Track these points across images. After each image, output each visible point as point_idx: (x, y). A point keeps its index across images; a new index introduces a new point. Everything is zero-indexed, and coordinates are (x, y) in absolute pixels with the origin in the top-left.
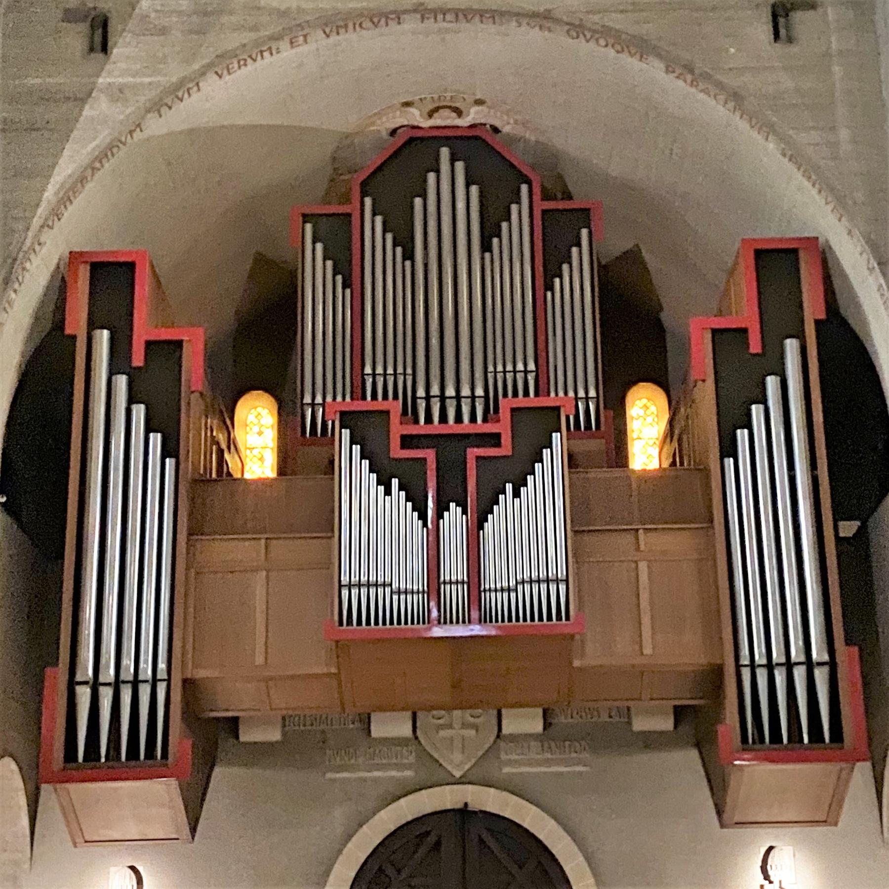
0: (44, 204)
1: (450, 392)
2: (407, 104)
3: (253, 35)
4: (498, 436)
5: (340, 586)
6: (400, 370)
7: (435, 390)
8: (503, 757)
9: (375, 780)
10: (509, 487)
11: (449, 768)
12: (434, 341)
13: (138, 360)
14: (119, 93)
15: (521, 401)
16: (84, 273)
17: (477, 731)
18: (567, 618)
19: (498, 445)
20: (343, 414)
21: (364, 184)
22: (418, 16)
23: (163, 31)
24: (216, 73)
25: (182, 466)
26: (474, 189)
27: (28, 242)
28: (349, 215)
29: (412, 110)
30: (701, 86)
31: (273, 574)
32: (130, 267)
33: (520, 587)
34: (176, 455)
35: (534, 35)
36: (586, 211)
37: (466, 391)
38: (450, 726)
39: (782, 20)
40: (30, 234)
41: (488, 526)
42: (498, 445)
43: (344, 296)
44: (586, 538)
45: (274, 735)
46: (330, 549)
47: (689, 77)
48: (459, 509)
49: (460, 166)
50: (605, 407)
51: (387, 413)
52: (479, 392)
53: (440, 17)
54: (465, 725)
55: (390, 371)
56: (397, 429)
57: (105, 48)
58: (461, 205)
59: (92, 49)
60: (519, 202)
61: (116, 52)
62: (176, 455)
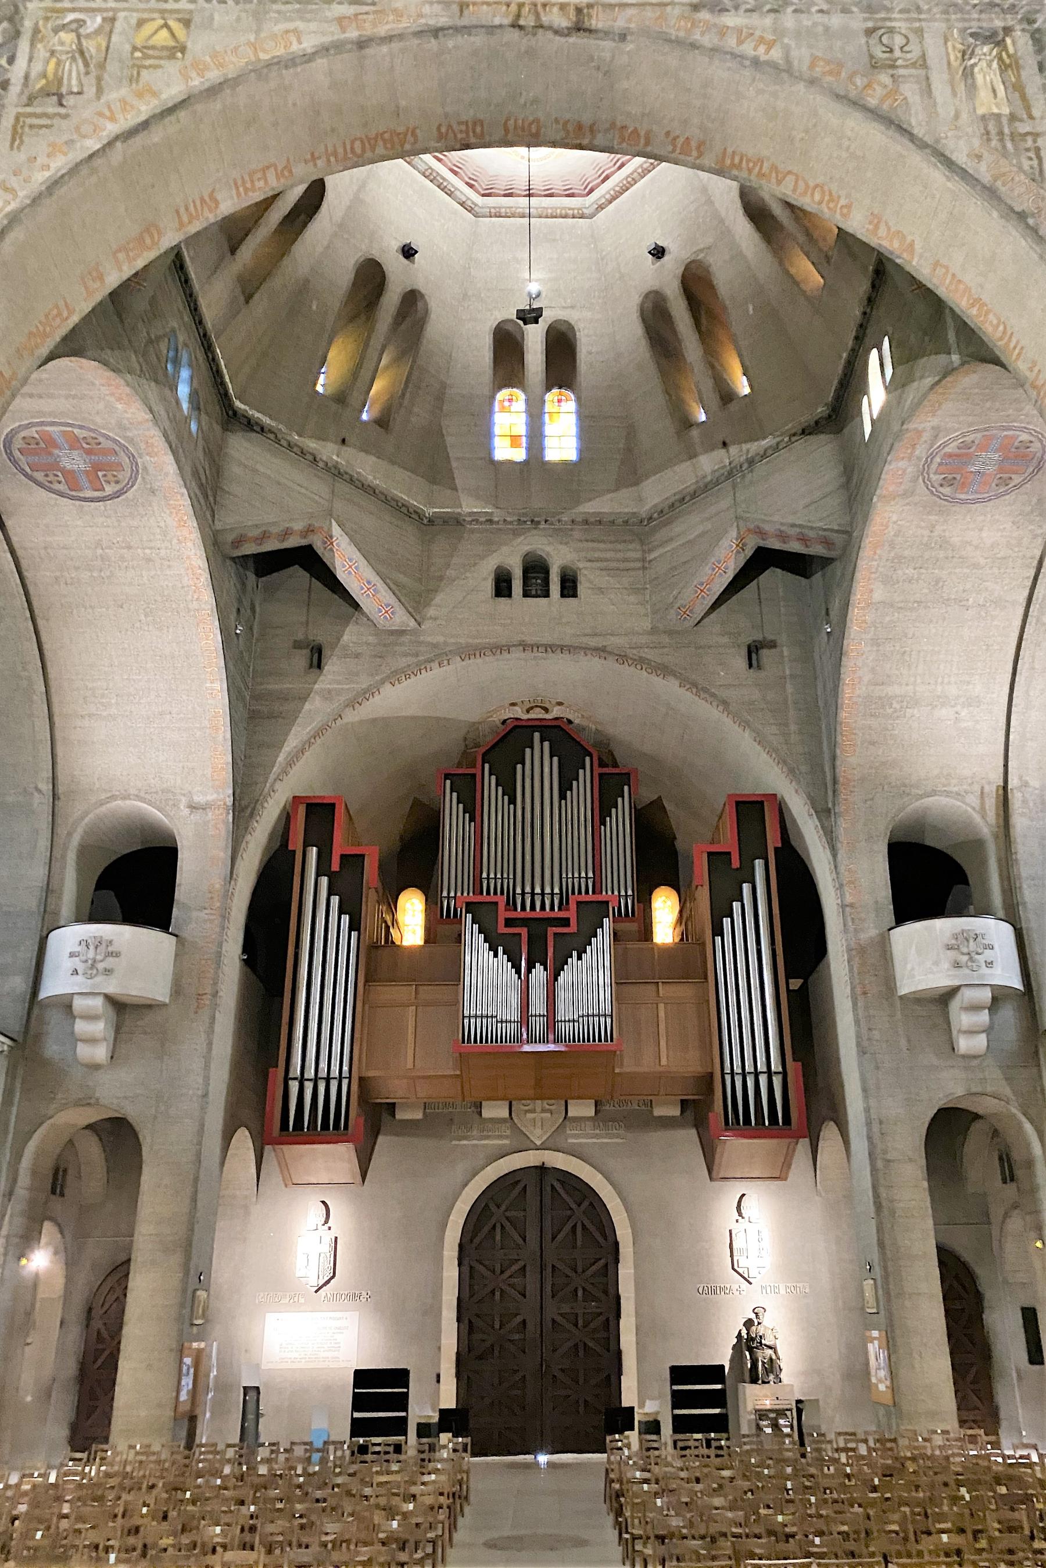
0: (277, 765)
1: (538, 890)
2: (513, 704)
3: (415, 660)
4: (568, 919)
6: (505, 876)
7: (528, 889)
8: (568, 1132)
9: (483, 1146)
10: (575, 953)
11: (532, 1138)
12: (528, 857)
13: (335, 867)
14: (328, 695)
15: (583, 898)
16: (302, 810)
18: (612, 1040)
19: (568, 925)
20: (468, 904)
21: (484, 755)
22: (521, 648)
23: (357, 656)
25: (362, 937)
26: (555, 759)
27: (266, 790)
28: (474, 776)
29: (516, 708)
30: (703, 695)
31: (420, 1009)
32: (333, 805)
33: (581, 1020)
34: (359, 930)
35: (595, 664)
36: (628, 774)
37: (548, 890)
38: (533, 1111)
39: (754, 656)
41: (561, 979)
42: (568, 925)
43: (470, 828)
44: (626, 989)
45: (419, 1115)
46: (457, 992)
47: (694, 690)
48: (542, 967)
49: (546, 744)
50: (638, 902)
51: (496, 903)
52: (557, 890)
53: (535, 649)
54: (543, 1111)
55: (499, 876)
56: (503, 914)
57: (319, 666)
58: (547, 770)
59: (311, 666)
60: (584, 768)
61: (328, 667)
62: (359, 930)
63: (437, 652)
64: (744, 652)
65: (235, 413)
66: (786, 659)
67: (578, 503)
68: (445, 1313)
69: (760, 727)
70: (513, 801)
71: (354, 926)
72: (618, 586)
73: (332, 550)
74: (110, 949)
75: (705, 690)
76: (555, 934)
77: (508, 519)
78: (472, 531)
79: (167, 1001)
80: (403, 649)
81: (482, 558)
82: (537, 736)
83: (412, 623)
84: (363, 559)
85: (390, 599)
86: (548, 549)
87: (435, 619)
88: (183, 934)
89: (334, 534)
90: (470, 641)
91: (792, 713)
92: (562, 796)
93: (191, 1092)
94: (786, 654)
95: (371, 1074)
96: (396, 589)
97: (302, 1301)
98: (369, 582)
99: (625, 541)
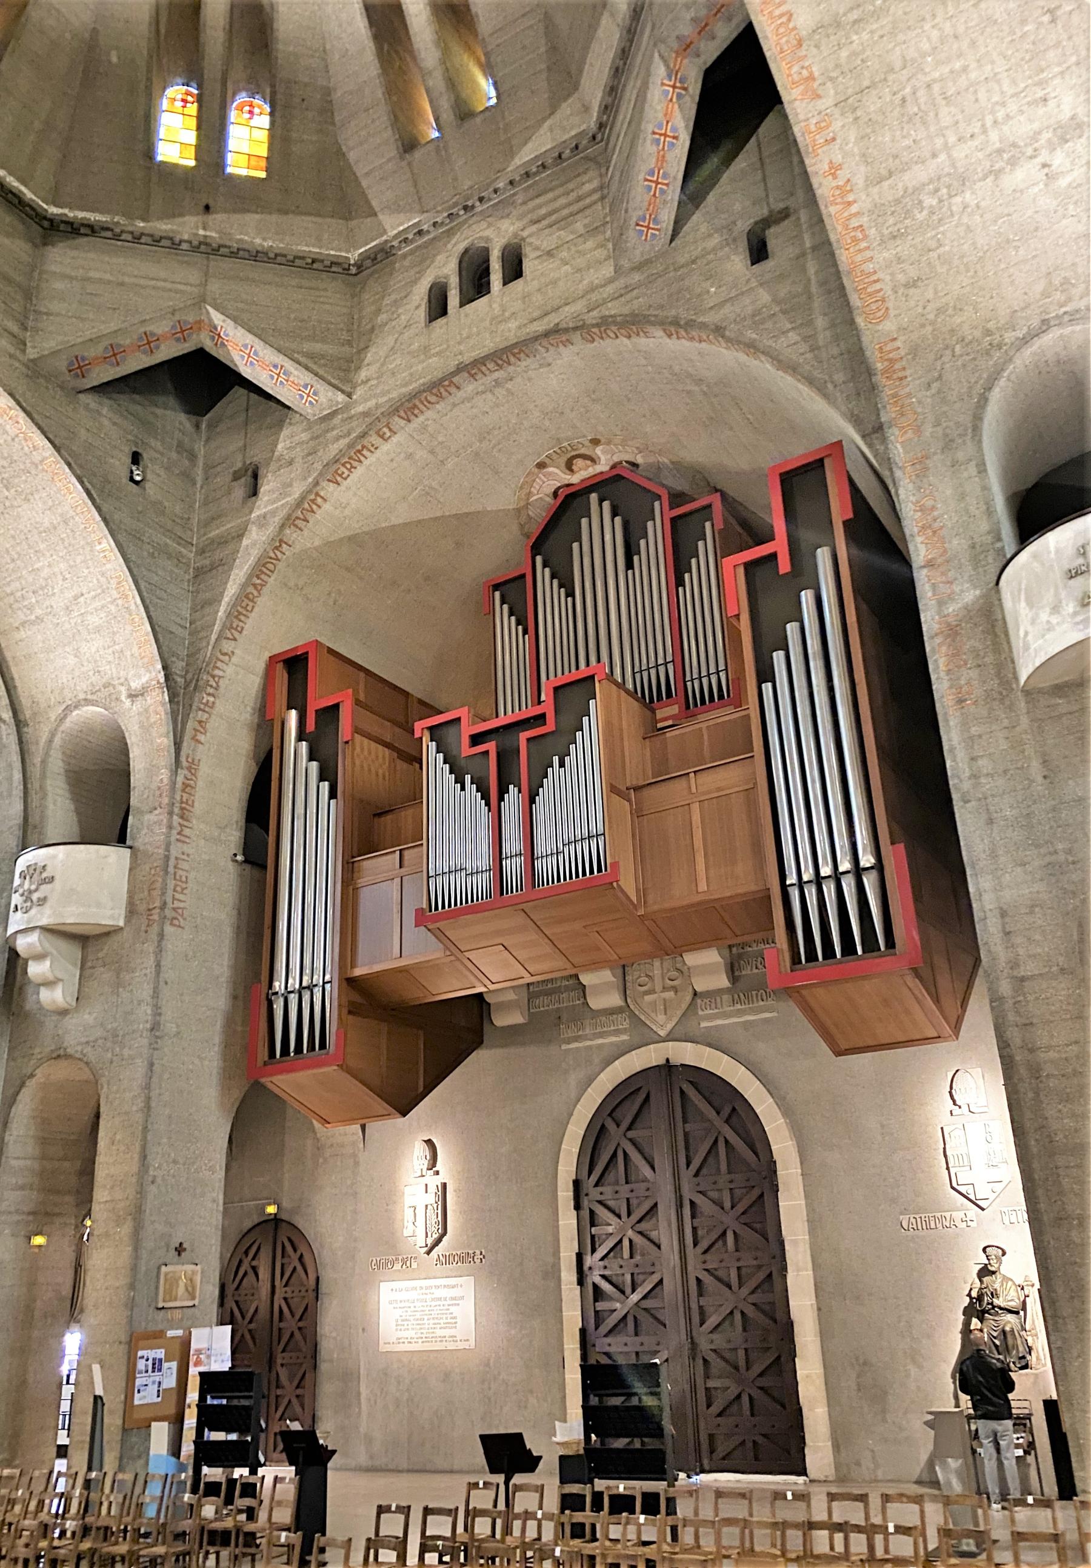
0: (218, 622)
5: (428, 877)
8: (700, 1013)
10: (556, 759)
17: (676, 992)
24: (329, 480)
27: (209, 655)
40: (210, 648)
45: (516, 1018)
48: (516, 789)
57: (254, 492)
63: (368, 420)
64: (743, 245)
65: (51, 221)
66: (804, 227)
67: (510, 153)
68: (564, 1275)
69: (770, 343)
70: (571, 594)
71: (333, 795)
72: (572, 237)
73: (223, 344)
74: (44, 875)
75: (690, 325)
76: (528, 740)
77: (439, 220)
78: (405, 256)
79: (121, 923)
80: (335, 433)
81: (415, 282)
82: (594, 497)
83: (341, 397)
84: (257, 340)
85: (306, 377)
86: (486, 233)
87: (368, 380)
88: (138, 844)
89: (216, 322)
90: (404, 390)
91: (817, 303)
92: (629, 565)
93: (141, 1026)
94: (803, 220)
95: (358, 972)
96: (310, 362)
97: (414, 1265)
98: (275, 366)
99: (579, 175)
